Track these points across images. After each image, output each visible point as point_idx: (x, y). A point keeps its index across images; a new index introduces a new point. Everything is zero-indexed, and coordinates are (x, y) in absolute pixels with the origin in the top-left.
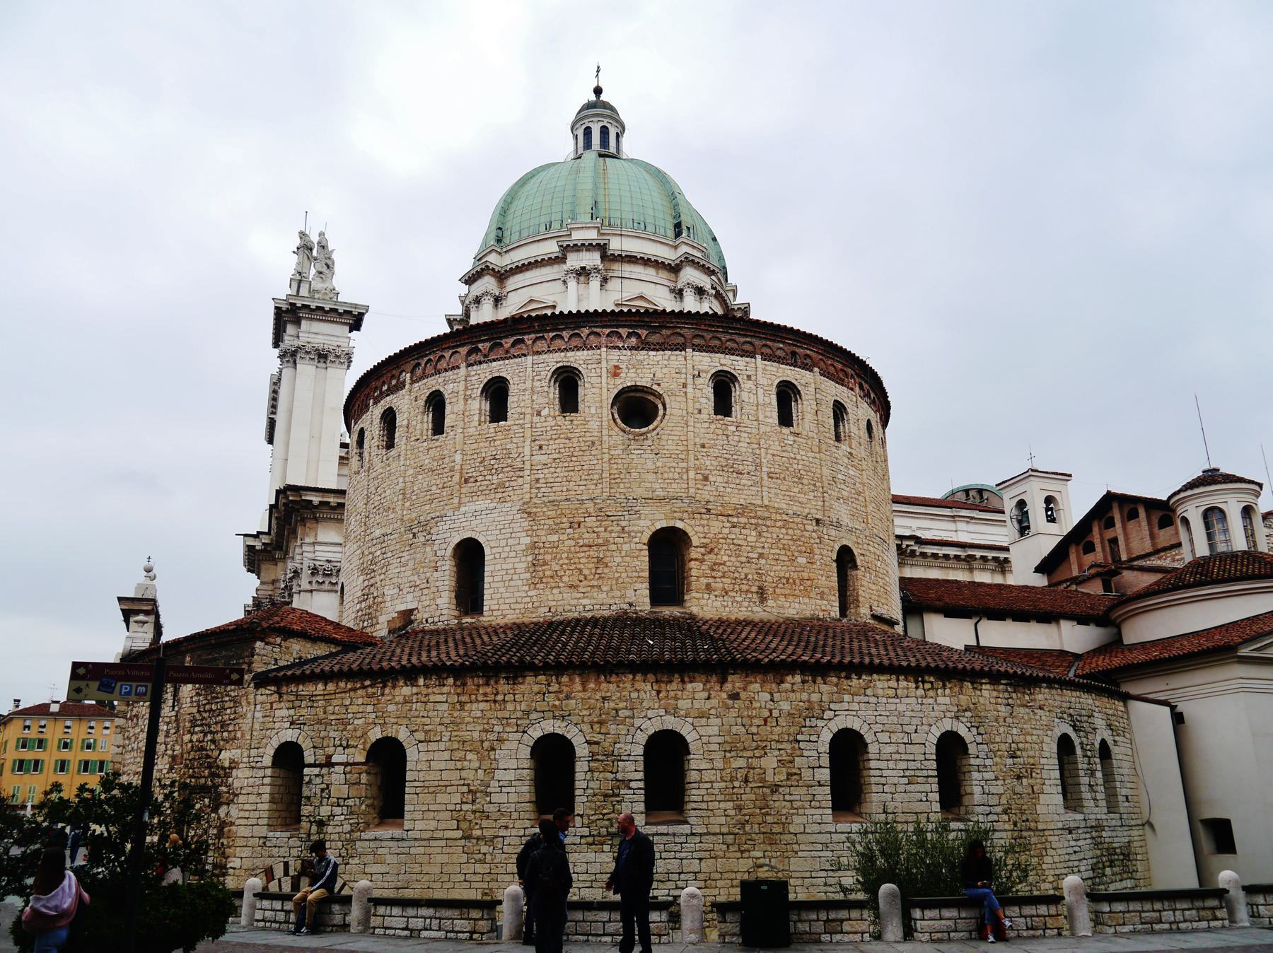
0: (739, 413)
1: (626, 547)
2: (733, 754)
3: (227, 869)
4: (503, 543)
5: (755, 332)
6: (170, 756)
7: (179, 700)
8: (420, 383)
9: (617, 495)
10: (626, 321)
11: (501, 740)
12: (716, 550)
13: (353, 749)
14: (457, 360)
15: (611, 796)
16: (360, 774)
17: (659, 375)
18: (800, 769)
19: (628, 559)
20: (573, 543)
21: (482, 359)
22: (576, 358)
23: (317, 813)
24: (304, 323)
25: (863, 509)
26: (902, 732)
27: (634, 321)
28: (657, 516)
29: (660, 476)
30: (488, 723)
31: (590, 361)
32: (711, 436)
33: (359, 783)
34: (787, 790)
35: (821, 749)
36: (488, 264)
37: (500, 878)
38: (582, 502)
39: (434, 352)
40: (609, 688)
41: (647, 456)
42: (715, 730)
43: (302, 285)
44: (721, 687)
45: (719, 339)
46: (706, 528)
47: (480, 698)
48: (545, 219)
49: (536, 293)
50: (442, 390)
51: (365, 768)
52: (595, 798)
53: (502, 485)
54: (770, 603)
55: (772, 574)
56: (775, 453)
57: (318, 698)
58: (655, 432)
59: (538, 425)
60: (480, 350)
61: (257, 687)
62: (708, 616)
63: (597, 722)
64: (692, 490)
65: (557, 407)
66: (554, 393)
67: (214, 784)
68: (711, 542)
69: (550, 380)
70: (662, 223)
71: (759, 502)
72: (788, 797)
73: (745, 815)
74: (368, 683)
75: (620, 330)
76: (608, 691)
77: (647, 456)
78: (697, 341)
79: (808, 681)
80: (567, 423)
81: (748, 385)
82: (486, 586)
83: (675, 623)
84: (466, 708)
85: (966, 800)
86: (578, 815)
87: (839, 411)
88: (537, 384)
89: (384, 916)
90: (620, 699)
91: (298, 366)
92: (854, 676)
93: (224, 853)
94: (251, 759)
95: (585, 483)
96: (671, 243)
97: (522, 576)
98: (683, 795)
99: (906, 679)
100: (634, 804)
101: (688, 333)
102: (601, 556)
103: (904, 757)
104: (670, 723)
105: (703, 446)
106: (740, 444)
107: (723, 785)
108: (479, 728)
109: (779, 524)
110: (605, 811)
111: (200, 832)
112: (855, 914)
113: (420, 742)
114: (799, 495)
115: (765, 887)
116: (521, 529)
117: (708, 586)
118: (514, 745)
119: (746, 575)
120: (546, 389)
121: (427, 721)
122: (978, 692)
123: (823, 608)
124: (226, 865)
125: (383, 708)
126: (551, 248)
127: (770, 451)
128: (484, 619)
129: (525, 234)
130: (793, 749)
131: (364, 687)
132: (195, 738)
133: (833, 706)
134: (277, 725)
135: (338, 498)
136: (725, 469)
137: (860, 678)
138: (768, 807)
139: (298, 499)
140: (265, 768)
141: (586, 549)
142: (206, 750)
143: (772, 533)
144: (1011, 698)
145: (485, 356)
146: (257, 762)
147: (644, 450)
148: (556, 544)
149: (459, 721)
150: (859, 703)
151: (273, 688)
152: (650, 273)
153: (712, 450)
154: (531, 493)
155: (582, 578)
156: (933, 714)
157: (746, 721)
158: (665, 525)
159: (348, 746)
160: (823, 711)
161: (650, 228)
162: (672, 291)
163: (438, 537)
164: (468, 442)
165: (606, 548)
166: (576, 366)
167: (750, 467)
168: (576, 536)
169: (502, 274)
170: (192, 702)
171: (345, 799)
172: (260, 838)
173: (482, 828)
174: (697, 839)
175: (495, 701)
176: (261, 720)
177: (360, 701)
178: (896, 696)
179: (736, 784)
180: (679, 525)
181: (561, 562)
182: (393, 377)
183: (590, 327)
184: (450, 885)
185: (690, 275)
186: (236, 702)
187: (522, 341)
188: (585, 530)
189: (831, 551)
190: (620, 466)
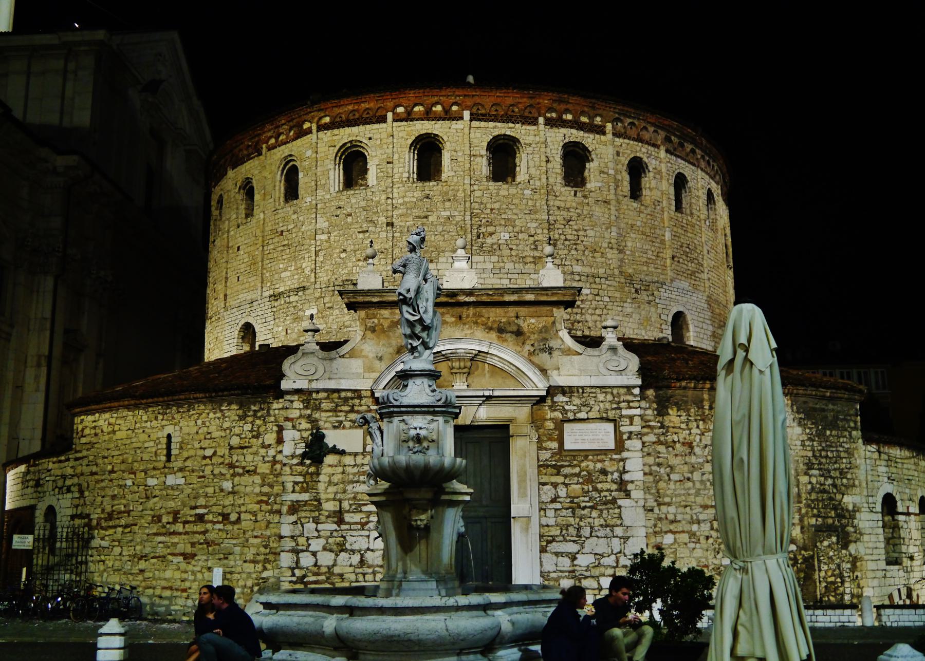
8: (621, 140)
14: (656, 140)
39: (639, 119)
67: (841, 524)
93: (859, 586)
124: (862, 594)
151: (875, 446)
170: (803, 445)
182: (583, 113)
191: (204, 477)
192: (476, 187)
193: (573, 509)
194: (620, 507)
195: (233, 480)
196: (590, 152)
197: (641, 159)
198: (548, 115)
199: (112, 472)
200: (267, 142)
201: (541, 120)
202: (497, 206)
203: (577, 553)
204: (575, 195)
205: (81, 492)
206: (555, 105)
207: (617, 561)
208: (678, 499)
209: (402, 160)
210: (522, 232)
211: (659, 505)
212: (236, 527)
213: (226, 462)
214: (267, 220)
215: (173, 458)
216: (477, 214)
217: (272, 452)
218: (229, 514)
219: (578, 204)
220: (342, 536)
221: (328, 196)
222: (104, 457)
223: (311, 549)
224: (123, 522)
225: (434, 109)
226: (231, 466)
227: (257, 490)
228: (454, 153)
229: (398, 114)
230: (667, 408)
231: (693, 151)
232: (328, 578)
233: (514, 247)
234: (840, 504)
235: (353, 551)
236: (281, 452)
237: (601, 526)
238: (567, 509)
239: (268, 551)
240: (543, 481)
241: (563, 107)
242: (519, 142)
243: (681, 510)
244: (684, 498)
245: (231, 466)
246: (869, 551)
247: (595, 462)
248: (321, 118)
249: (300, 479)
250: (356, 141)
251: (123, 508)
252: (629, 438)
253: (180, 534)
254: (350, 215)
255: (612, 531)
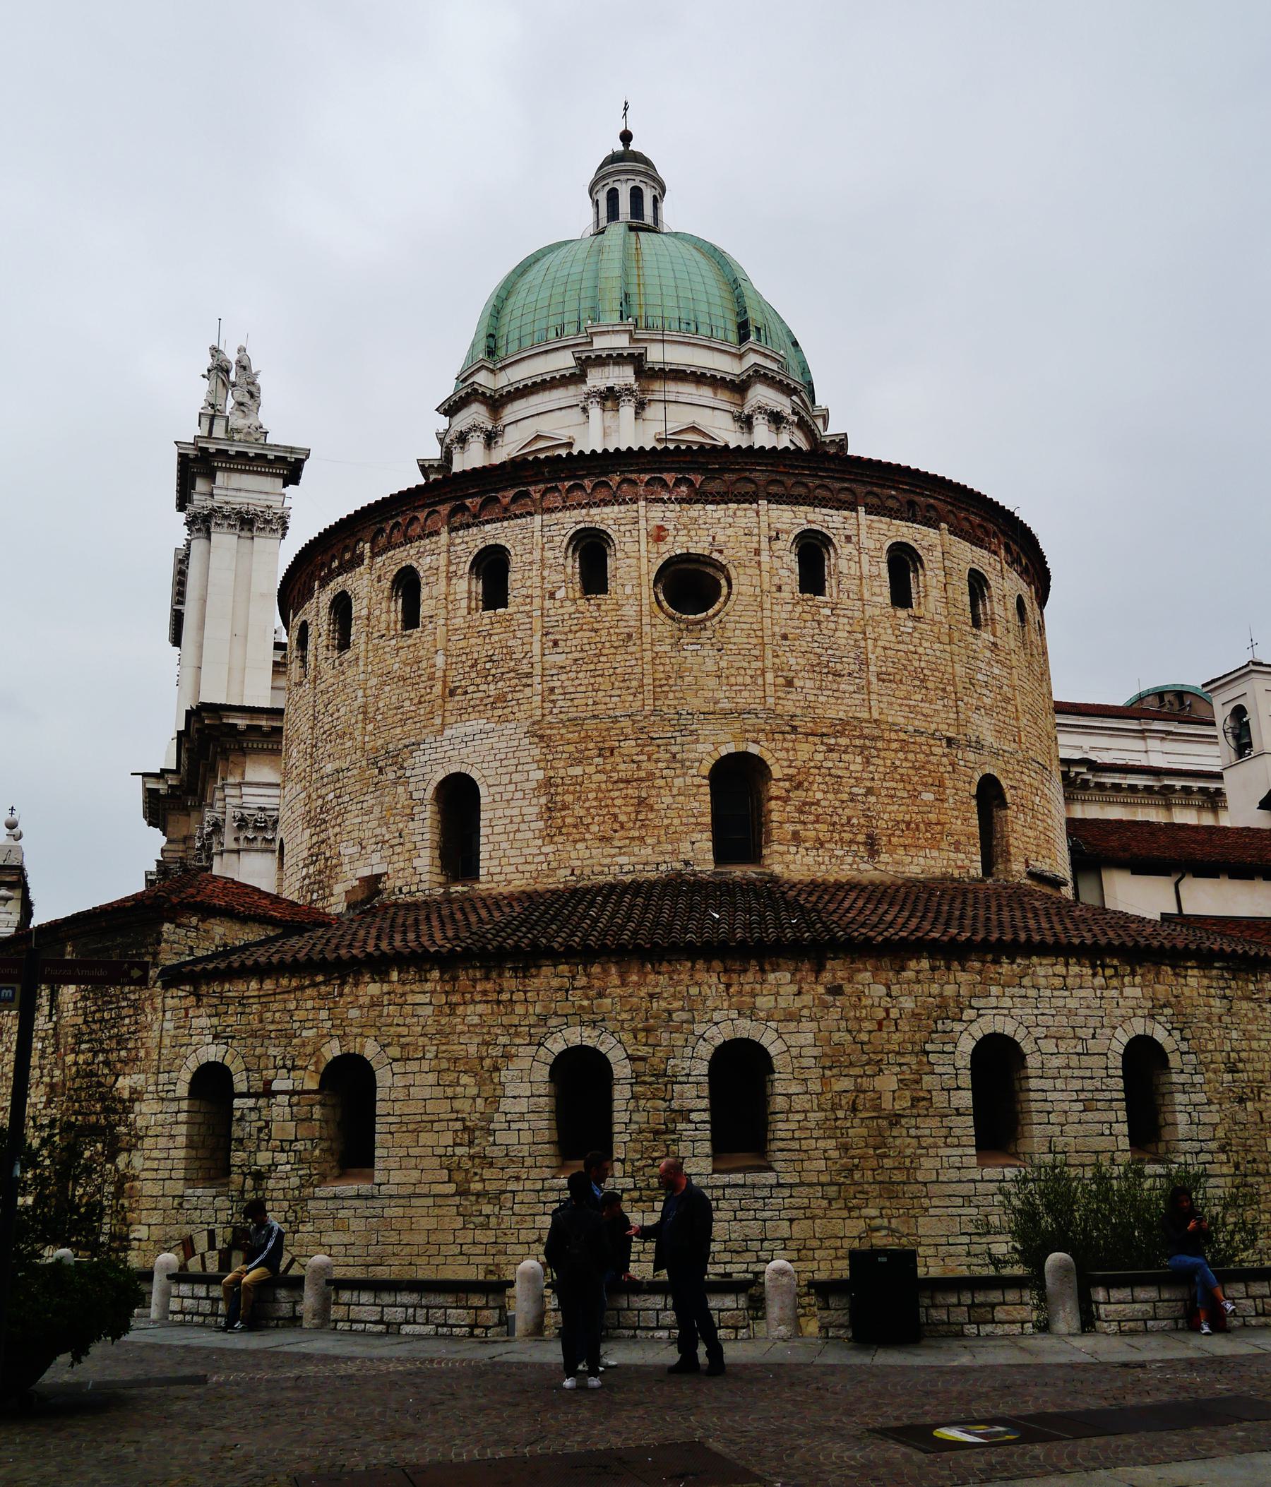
0: (835, 590)
1: (678, 782)
2: (835, 1071)
3: (129, 1241)
4: (506, 779)
5: (856, 474)
6: (47, 1085)
7: (58, 1006)
8: (384, 557)
9: (665, 709)
10: (673, 462)
11: (507, 1057)
12: (806, 784)
13: (302, 1072)
14: (435, 523)
15: (664, 1132)
16: (311, 1106)
17: (721, 538)
18: (929, 1091)
19: (681, 798)
20: (604, 777)
21: (471, 521)
22: (605, 517)
23: (252, 1161)
24: (220, 477)
25: (1014, 722)
26: (1075, 1037)
27: (685, 462)
28: (722, 738)
29: (725, 681)
30: (489, 1033)
31: (623, 521)
32: (796, 623)
33: (310, 1119)
34: (913, 1122)
35: (960, 1064)
36: (476, 386)
37: (510, 1249)
38: (615, 720)
39: (403, 512)
40: (658, 981)
41: (705, 653)
42: (810, 1038)
43: (216, 421)
44: (816, 978)
45: (806, 485)
46: (791, 753)
47: (478, 998)
48: (554, 321)
49: (545, 425)
50: (415, 565)
51: (318, 1097)
52: (641, 1137)
53: (501, 698)
54: (884, 857)
55: (886, 816)
56: (888, 645)
57: (251, 1001)
58: (717, 619)
59: (551, 612)
60: (467, 508)
61: (166, 987)
62: (796, 877)
63: (643, 1030)
64: (771, 701)
65: (578, 587)
66: (573, 566)
68: (799, 773)
69: (567, 549)
70: (721, 323)
71: (866, 715)
72: (913, 1132)
73: (853, 1157)
74: (320, 978)
75: (665, 476)
76: (657, 986)
77: (705, 653)
78: (773, 489)
79: (939, 968)
80: (591, 608)
81: (847, 549)
82: (483, 840)
83: (748, 887)
84: (458, 1012)
85: (1166, 1133)
86: (618, 1160)
87: (977, 583)
88: (549, 554)
89: (349, 1305)
90: (674, 995)
91: (213, 536)
92: (1004, 960)
93: (124, 1219)
94: (160, 1088)
95: (618, 692)
96: (733, 350)
97: (533, 825)
98: (766, 1130)
99: (1079, 964)
100: (697, 1144)
101: (760, 477)
102: (644, 795)
103: (1077, 1073)
104: (746, 1029)
105: (785, 637)
106: (838, 634)
107: (821, 1115)
108: (477, 1040)
109: (894, 745)
110: (656, 1154)
111: (90, 1190)
112: (1011, 1296)
113: (395, 1060)
114: (922, 705)
115: (884, 1259)
116: (530, 760)
117: (795, 834)
118: (526, 1064)
119: (849, 819)
120: (561, 561)
121: (404, 1031)
122: (1182, 981)
123: (959, 863)
124: (128, 1235)
125: (342, 1013)
126: (564, 361)
127: (880, 643)
128: (481, 886)
129: (527, 342)
130: (920, 1063)
131: (314, 985)
132: (81, 1059)
133: (974, 1003)
134: (195, 1039)
135: (272, 720)
136: (817, 669)
137: (1012, 962)
138: (885, 1145)
139: (217, 722)
140: (179, 1099)
141: (622, 785)
142: (97, 1076)
143: (884, 759)
144: (1229, 987)
145: (475, 517)
146: (168, 1091)
147: (702, 645)
148: (580, 780)
149: (448, 1030)
150: (1012, 998)
151: (188, 988)
152: (704, 394)
153: (797, 643)
154: (543, 708)
155: (617, 826)
156: (1118, 1012)
157: (852, 1025)
158: (733, 750)
159: (294, 1068)
160: (962, 1010)
161: (704, 330)
162: (737, 418)
163: (414, 773)
164: (453, 638)
165: (649, 783)
166: (603, 527)
167: (852, 666)
168: (608, 767)
169: (497, 400)
170: (76, 1009)
171: (291, 1142)
172: (174, 1197)
173: (483, 1181)
174: (787, 1192)
175: (499, 1002)
176: (172, 1032)
177: (310, 1004)
178: (1065, 988)
179: (840, 1114)
180: (754, 749)
181: (587, 805)
182: (346, 549)
183: (622, 472)
184: (440, 1260)
185: (762, 395)
186: (137, 1008)
187: (527, 494)
188: (619, 759)
189: (970, 783)
190: (668, 668)
197: (410, 567)
234: (111, 1092)
246: (155, 1165)
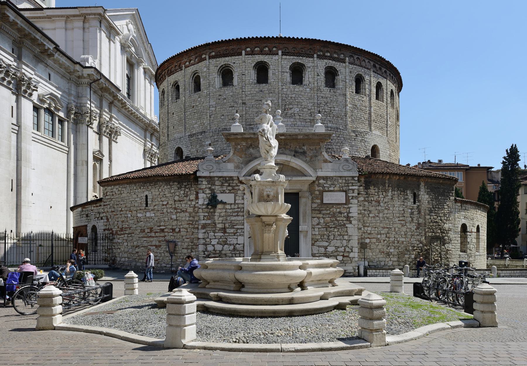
7: (419, 201)
8: (353, 66)
39: (361, 56)
170: (428, 203)
182: (335, 53)
191: (163, 213)
192: (284, 87)
193: (326, 228)
194: (347, 227)
195: (176, 215)
196: (337, 71)
197: (361, 75)
198: (319, 53)
199: (121, 211)
200: (185, 64)
201: (315, 56)
202: (294, 96)
203: (328, 246)
204: (330, 91)
205: (108, 219)
206: (322, 49)
207: (345, 250)
208: (372, 225)
209: (249, 74)
210: (305, 108)
211: (364, 227)
212: (178, 234)
213: (173, 207)
214: (186, 100)
215: (149, 205)
216: (285, 99)
217: (193, 203)
218: (175, 229)
219: (331, 95)
220: (226, 238)
221: (215, 90)
222: (117, 205)
223: (212, 243)
224: (127, 232)
225: (265, 49)
226: (175, 209)
227: (187, 219)
228: (273, 71)
229: (248, 52)
230: (369, 186)
231: (385, 72)
232: (219, 255)
233: (301, 115)
235: (230, 245)
236: (198, 203)
237: (339, 235)
238: (324, 228)
239: (193, 244)
240: (314, 216)
241: (326, 49)
242: (305, 66)
243: (373, 229)
244: (375, 224)
245: (175, 209)
247: (336, 209)
248: (210, 53)
249: (207, 214)
250: (227, 64)
251: (127, 226)
252: (352, 199)
253: (154, 237)
254: (225, 99)
255: (343, 237)
